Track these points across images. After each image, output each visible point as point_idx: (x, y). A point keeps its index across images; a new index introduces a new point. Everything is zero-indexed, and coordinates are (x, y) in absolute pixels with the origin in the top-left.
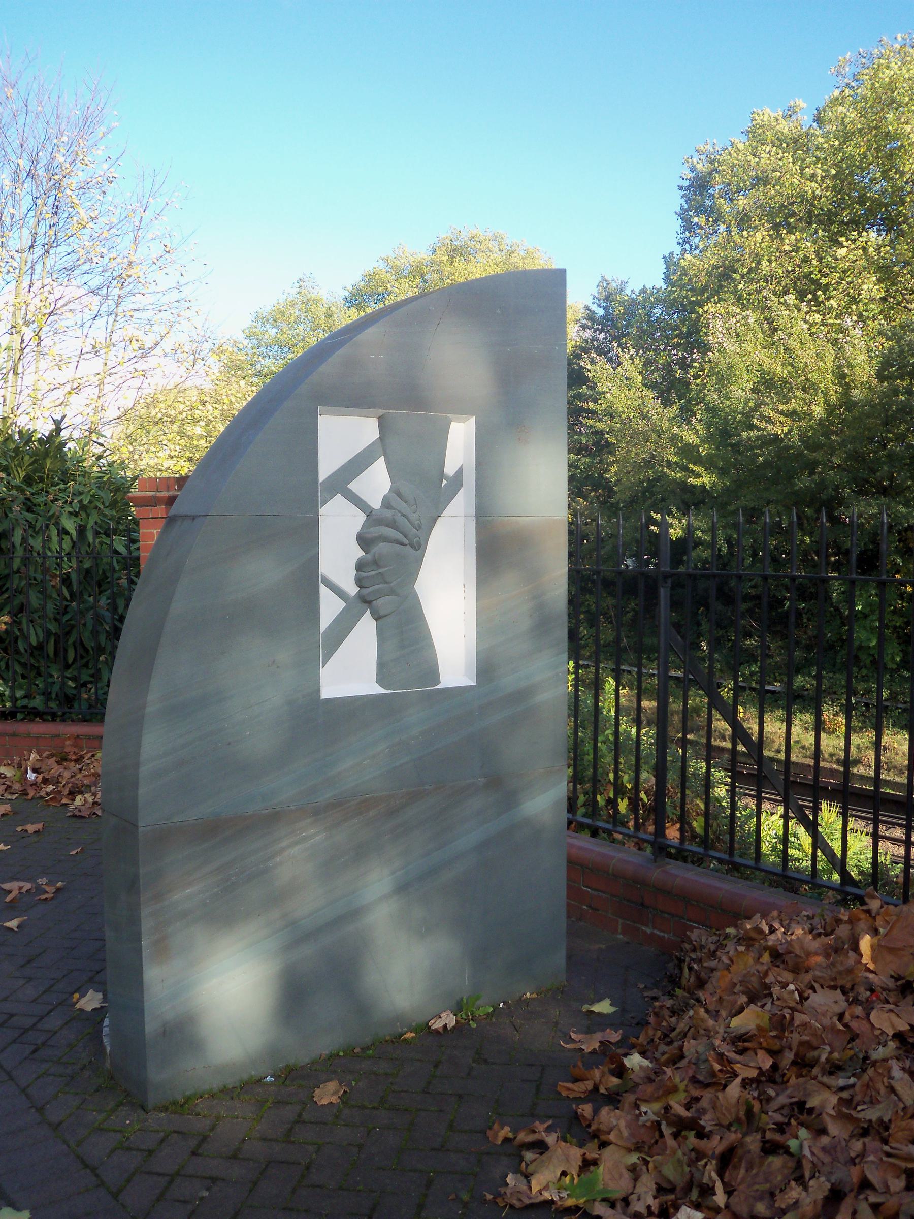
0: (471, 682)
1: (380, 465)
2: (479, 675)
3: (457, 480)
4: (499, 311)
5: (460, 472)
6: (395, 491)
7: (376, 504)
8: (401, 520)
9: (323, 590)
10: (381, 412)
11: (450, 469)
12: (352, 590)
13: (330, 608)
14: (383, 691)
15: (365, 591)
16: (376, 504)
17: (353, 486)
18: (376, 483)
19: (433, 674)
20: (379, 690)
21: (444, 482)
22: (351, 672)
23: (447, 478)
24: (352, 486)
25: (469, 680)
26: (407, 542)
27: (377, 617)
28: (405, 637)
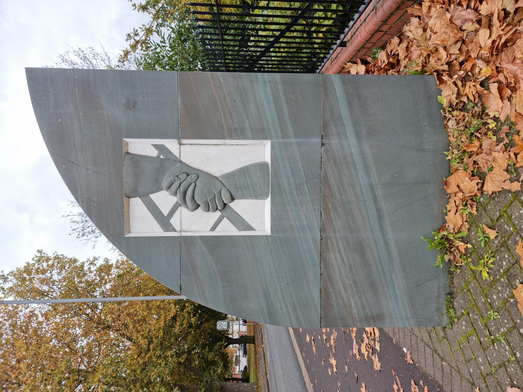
0: (268, 144)
1: (154, 197)
2: (266, 139)
3: (160, 148)
4: (59, 120)
5: (155, 146)
6: (169, 188)
7: (174, 200)
8: (182, 188)
9: (217, 233)
10: (125, 199)
11: (154, 153)
12: (218, 214)
13: (227, 229)
14: (269, 199)
15: (219, 208)
16: (174, 200)
17: (166, 213)
18: (164, 200)
19: (263, 166)
20: (268, 201)
21: (162, 157)
22: (258, 215)
23: (158, 157)
24: (166, 213)
25: (268, 144)
26: (193, 184)
27: (233, 199)
28: (244, 182)
